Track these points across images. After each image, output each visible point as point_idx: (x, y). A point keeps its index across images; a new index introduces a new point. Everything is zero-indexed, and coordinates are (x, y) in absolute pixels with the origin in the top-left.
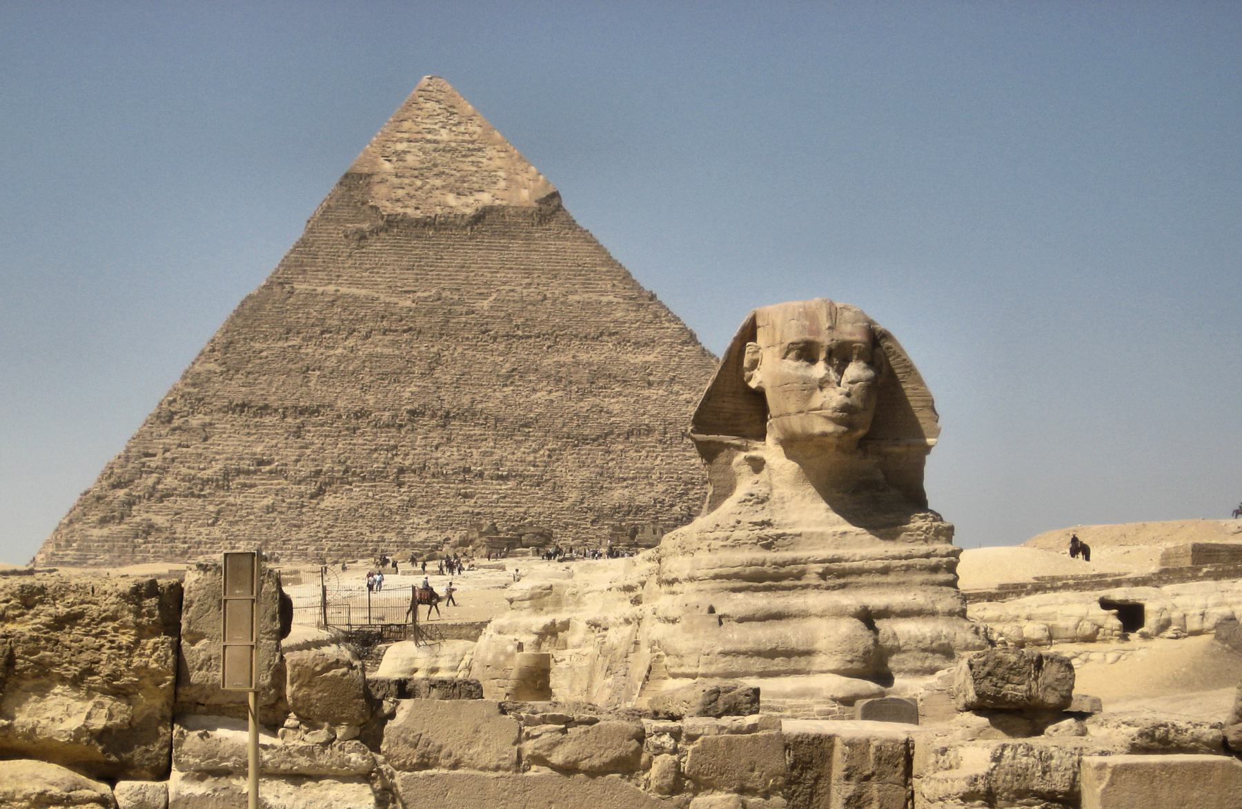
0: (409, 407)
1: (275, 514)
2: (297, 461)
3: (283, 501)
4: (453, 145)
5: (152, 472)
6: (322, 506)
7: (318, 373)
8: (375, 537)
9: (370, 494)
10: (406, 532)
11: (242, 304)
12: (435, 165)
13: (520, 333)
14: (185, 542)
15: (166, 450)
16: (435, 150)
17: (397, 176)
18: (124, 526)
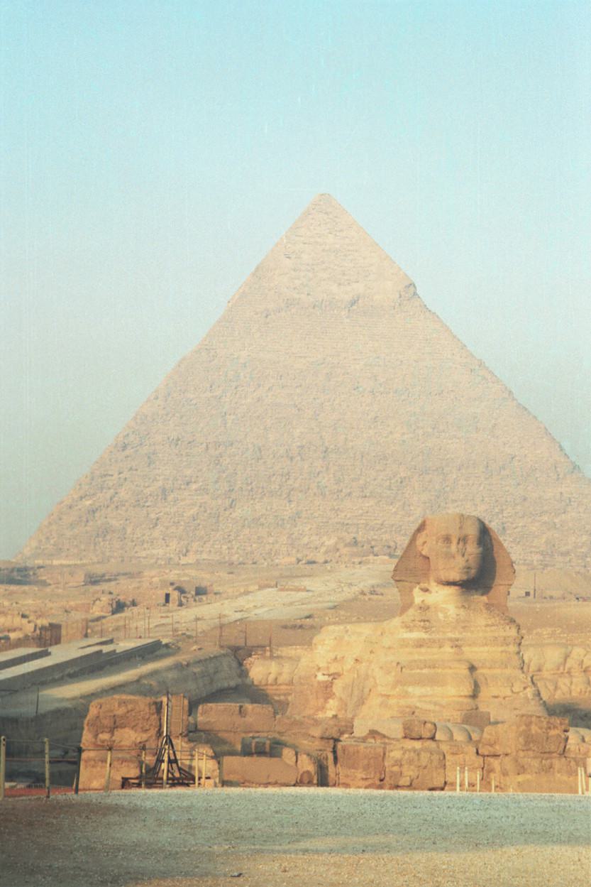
0: (299, 444)
1: (198, 521)
2: (216, 482)
3: (205, 511)
4: (338, 246)
5: (109, 488)
6: (234, 515)
7: (232, 417)
8: (271, 540)
9: (269, 508)
10: (293, 536)
11: (179, 366)
12: (323, 262)
13: (382, 389)
14: (133, 541)
15: (120, 473)
16: (323, 250)
17: (294, 270)
18: (87, 528)
